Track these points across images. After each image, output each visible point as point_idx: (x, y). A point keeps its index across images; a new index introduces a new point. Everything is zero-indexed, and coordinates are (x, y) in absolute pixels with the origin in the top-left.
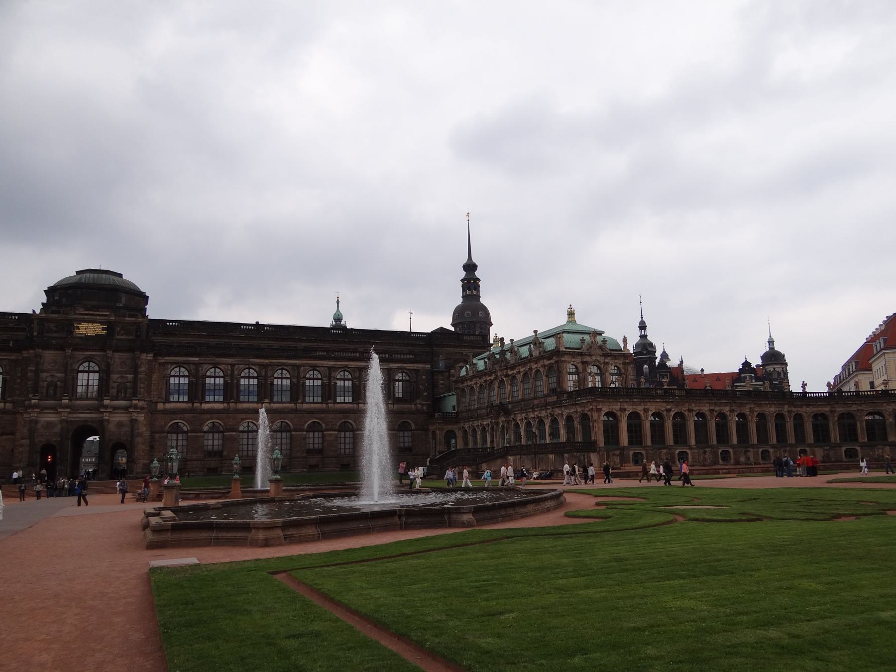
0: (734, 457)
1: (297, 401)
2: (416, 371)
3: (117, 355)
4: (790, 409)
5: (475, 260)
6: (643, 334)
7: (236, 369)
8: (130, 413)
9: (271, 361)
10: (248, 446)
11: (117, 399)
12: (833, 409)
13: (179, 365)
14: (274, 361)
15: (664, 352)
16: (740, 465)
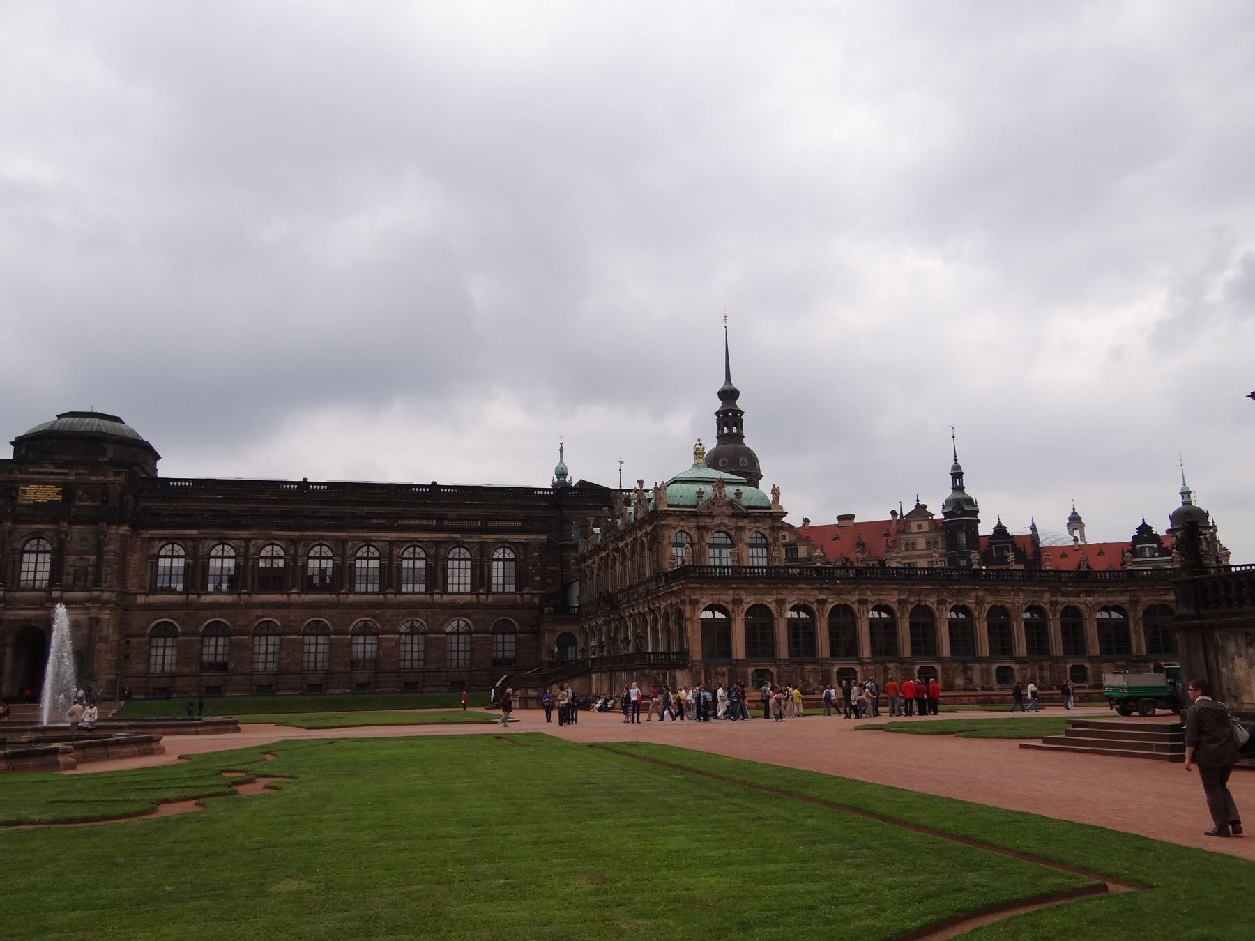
0: (943, 678)
1: (341, 589)
2: (525, 545)
3: (76, 528)
4: (1054, 599)
5: (736, 383)
6: (958, 484)
7: (253, 546)
8: (87, 608)
9: (303, 533)
10: (458, 653)
11: (73, 591)
12: (1135, 599)
13: (171, 541)
14: (308, 533)
15: (1074, 513)
16: (954, 690)
